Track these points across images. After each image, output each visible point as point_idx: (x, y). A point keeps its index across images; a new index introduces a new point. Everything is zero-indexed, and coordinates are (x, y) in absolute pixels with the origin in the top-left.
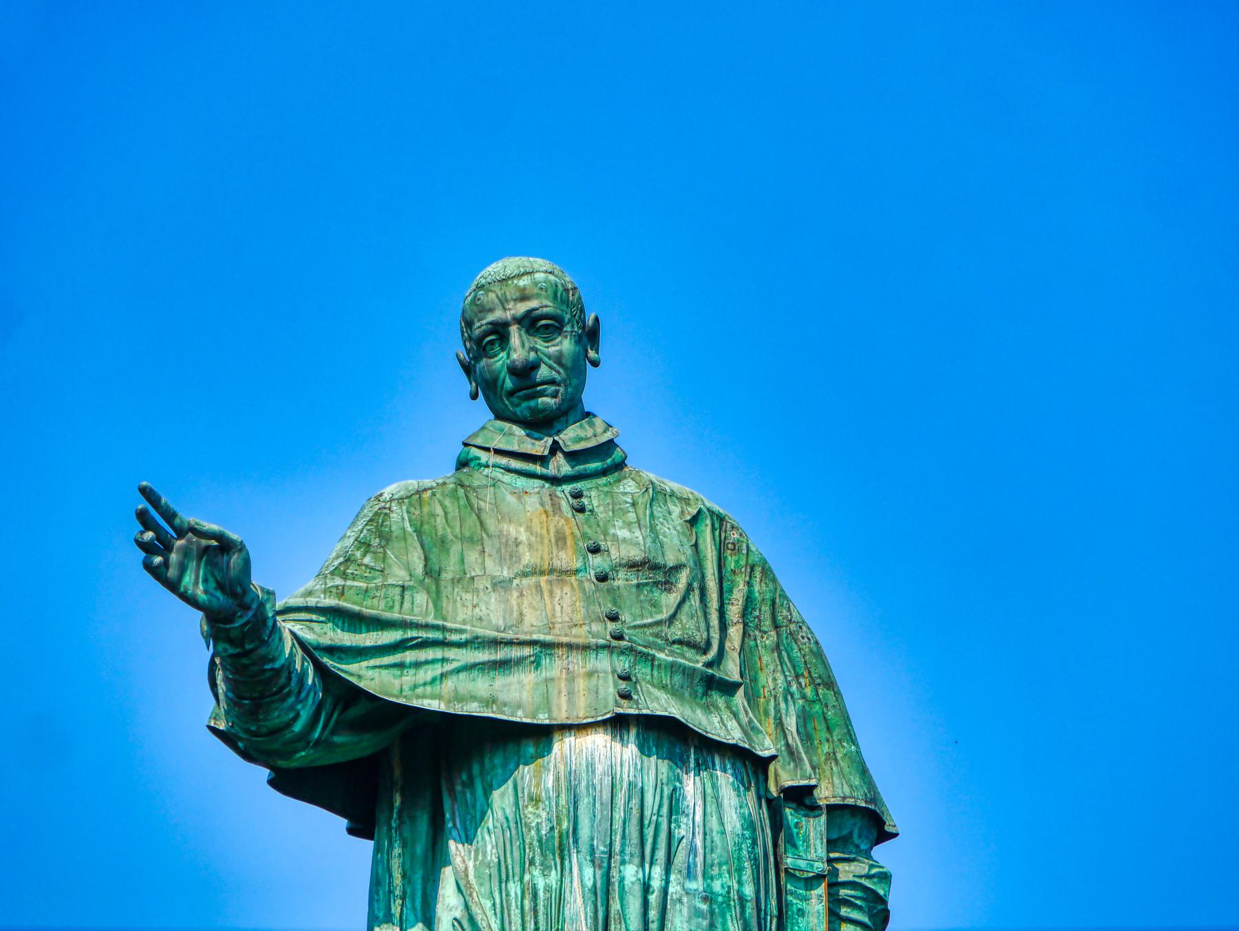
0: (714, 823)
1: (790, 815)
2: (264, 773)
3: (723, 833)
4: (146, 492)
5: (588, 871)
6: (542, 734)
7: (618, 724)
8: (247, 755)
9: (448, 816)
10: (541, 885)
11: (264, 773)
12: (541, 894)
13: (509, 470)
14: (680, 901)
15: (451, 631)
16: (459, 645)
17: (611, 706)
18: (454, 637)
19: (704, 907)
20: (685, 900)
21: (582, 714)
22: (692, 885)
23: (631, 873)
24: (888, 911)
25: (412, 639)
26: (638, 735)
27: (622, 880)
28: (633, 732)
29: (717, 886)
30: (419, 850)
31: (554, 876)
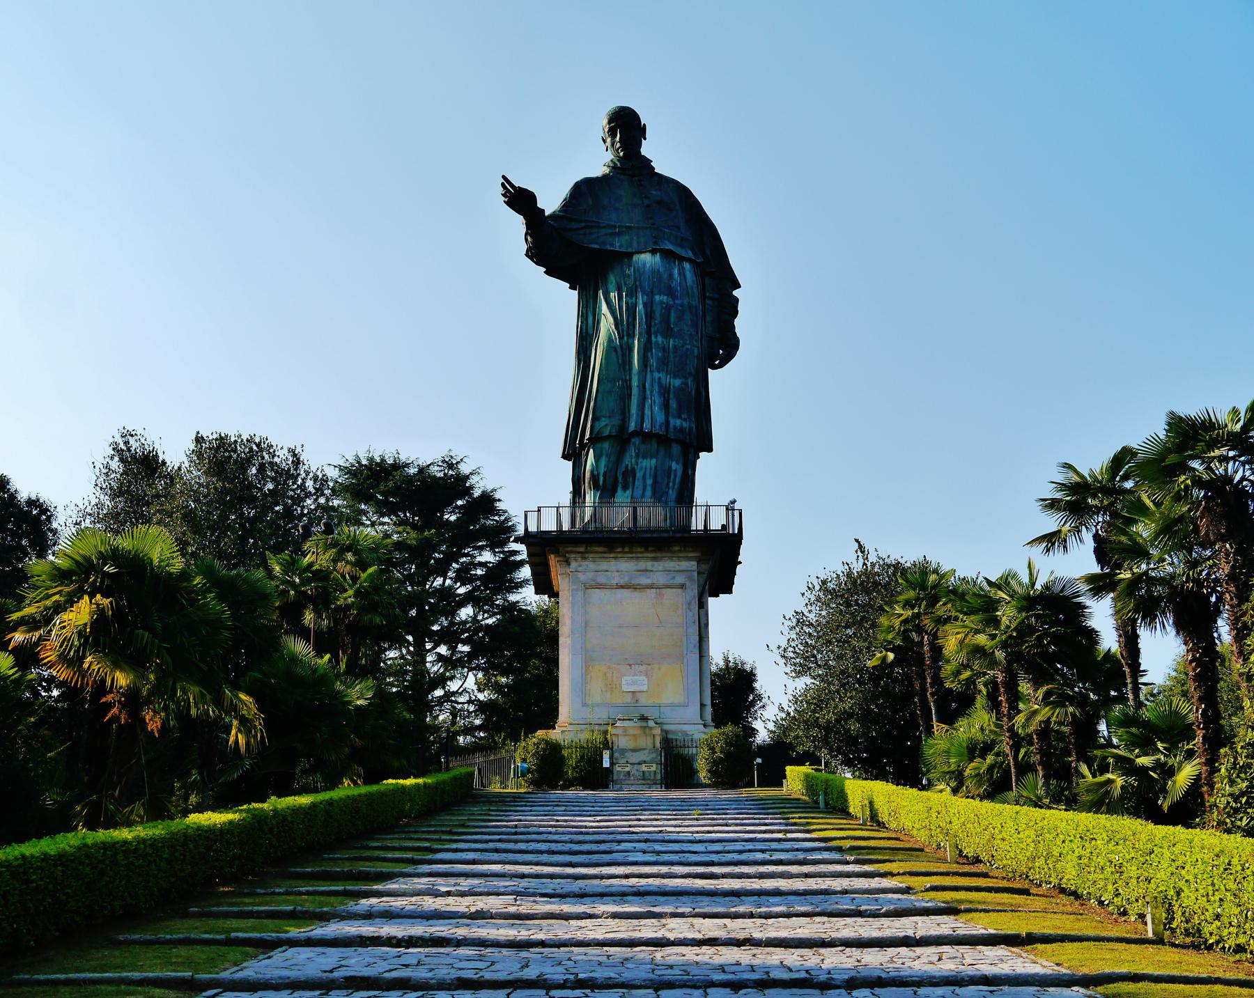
1: (707, 281)
4: (504, 177)
7: (653, 252)
8: (537, 263)
23: (657, 298)
29: (685, 302)
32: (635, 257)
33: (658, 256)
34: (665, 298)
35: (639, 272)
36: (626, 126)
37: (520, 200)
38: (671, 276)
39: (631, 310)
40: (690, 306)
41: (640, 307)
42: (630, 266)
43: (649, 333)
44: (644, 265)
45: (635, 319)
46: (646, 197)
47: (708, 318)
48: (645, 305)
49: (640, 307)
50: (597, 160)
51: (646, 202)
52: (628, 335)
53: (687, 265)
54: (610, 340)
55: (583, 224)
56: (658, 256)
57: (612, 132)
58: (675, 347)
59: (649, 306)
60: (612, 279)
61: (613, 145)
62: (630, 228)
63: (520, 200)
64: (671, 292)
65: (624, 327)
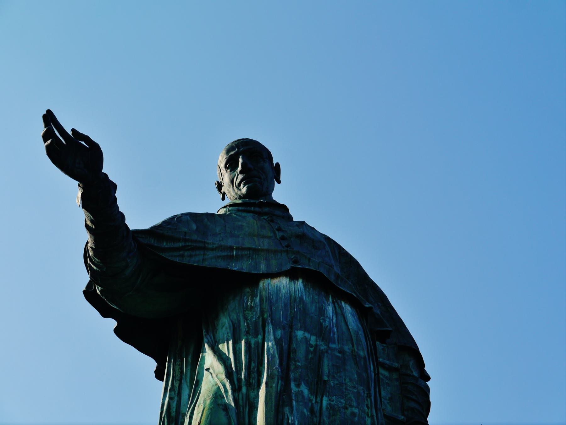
0: (343, 324)
2: (112, 323)
3: (348, 329)
5: (279, 333)
6: (253, 280)
7: (293, 275)
9: (204, 331)
10: (253, 341)
11: (112, 323)
12: (253, 346)
13: (238, 211)
14: (327, 352)
15: (208, 244)
16: (213, 249)
17: (287, 267)
18: (210, 246)
19: (340, 355)
20: (330, 352)
21: (275, 270)
22: (333, 346)
23: (300, 334)
24: (430, 403)
25: (188, 246)
26: (303, 282)
27: (296, 336)
28: (300, 281)
29: (347, 348)
30: (190, 359)
31: (260, 337)
32: (263, 284)
33: (300, 284)
34: (313, 340)
35: (270, 300)
36: (253, 162)
37: (74, 154)
38: (322, 312)
39: (256, 354)
40: (355, 356)
41: (269, 345)
42: (253, 296)
43: (285, 378)
44: (278, 290)
45: (261, 363)
46: (279, 230)
47: (383, 393)
48: (278, 342)
49: (269, 345)
50: (210, 200)
51: (279, 234)
52: (249, 384)
53: (347, 308)
54: (217, 396)
55: (181, 244)
56: (300, 284)
57: (231, 164)
58: (331, 407)
59: (286, 351)
60: (224, 322)
61: (232, 181)
62: (256, 251)
63: (74, 154)
64: (322, 333)
65: (242, 382)
